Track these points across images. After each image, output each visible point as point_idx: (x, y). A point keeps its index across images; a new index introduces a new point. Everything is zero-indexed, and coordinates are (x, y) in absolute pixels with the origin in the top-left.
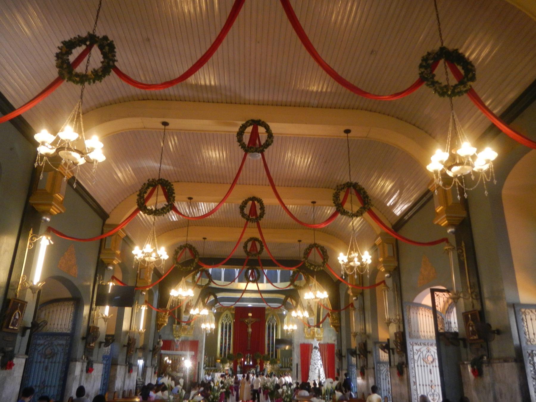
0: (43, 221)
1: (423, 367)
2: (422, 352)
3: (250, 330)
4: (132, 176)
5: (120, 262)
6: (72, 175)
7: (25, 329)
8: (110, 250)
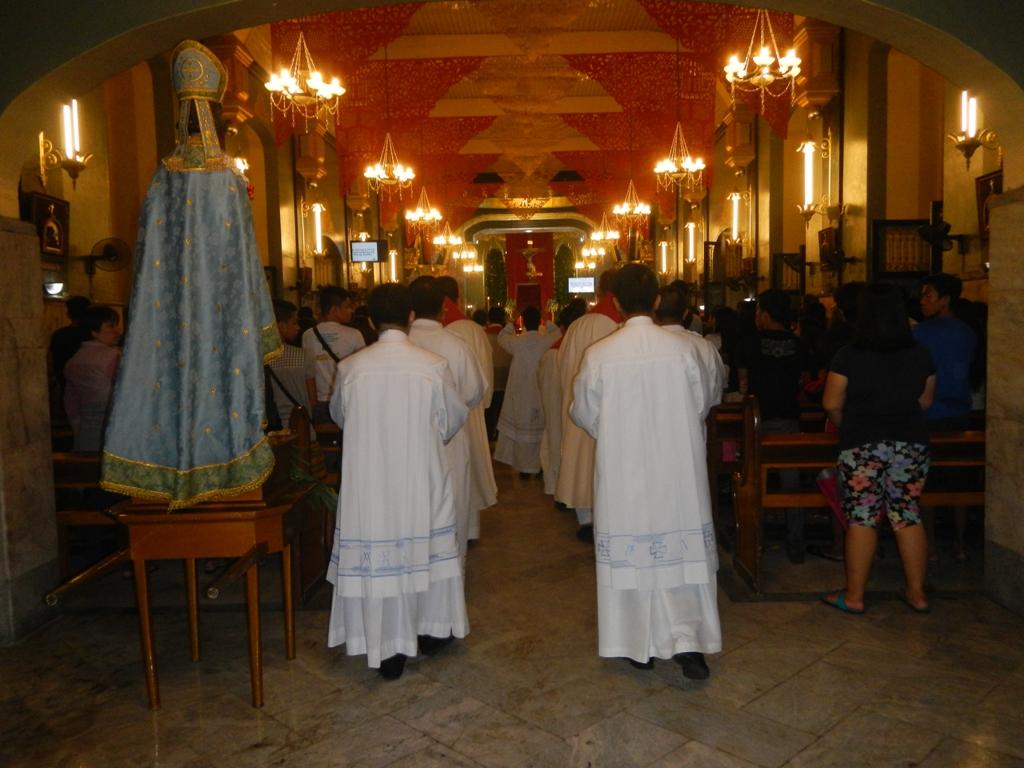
0: (229, 133)
6: (251, 60)
7: (315, 292)
8: (357, 194)
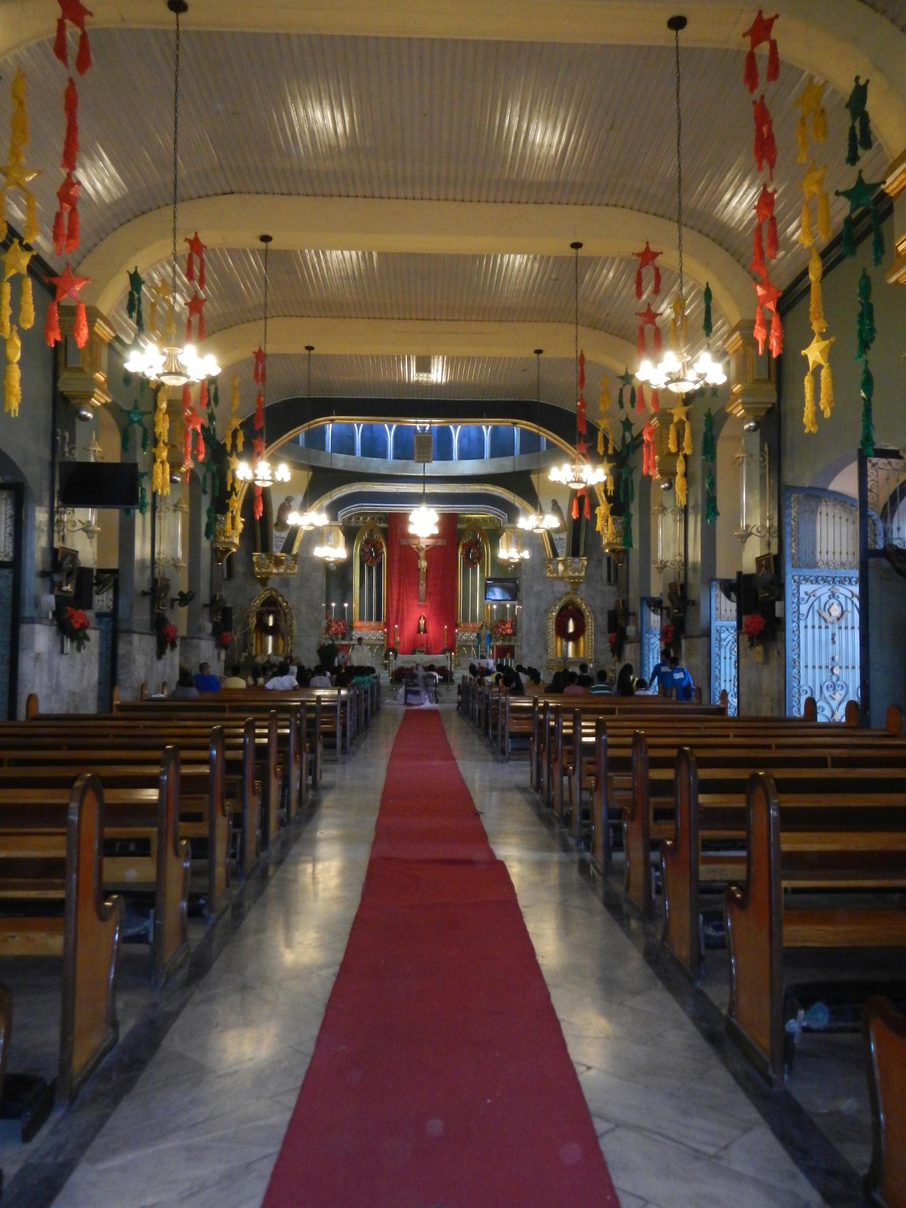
1: (817, 630)
2: (819, 598)
3: (423, 564)
4: (112, 177)
5: (109, 400)
8: (81, 370)
